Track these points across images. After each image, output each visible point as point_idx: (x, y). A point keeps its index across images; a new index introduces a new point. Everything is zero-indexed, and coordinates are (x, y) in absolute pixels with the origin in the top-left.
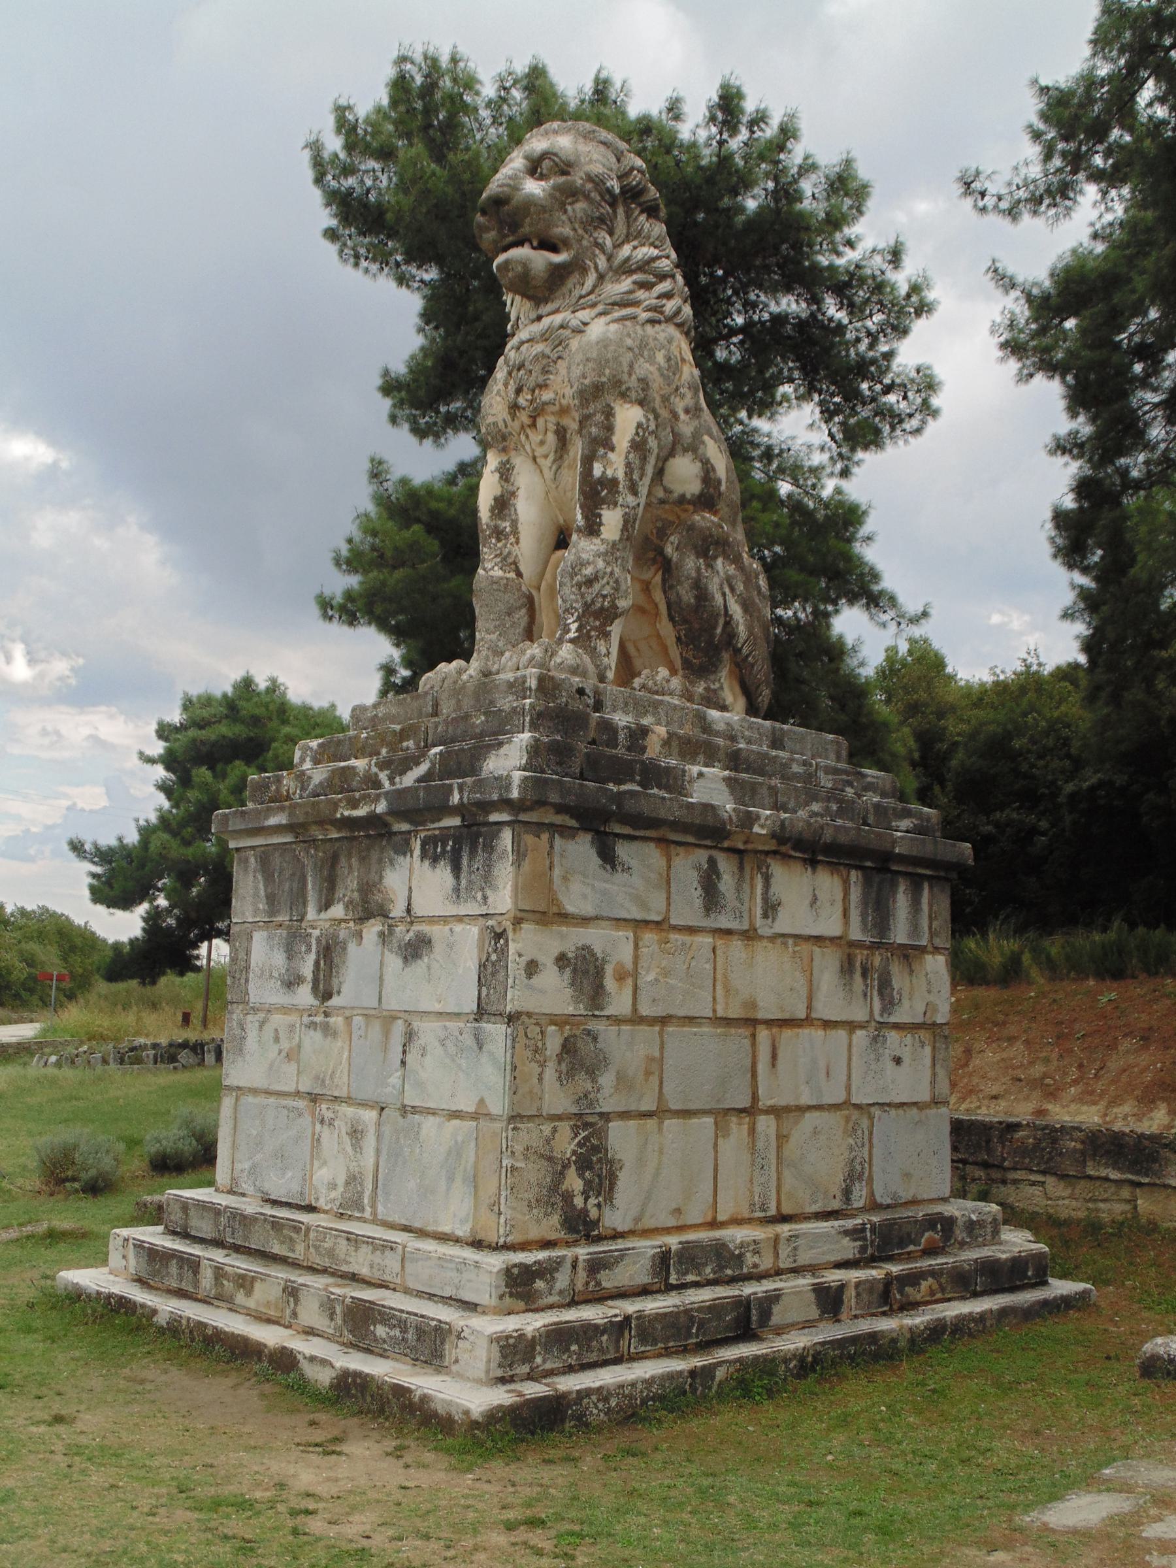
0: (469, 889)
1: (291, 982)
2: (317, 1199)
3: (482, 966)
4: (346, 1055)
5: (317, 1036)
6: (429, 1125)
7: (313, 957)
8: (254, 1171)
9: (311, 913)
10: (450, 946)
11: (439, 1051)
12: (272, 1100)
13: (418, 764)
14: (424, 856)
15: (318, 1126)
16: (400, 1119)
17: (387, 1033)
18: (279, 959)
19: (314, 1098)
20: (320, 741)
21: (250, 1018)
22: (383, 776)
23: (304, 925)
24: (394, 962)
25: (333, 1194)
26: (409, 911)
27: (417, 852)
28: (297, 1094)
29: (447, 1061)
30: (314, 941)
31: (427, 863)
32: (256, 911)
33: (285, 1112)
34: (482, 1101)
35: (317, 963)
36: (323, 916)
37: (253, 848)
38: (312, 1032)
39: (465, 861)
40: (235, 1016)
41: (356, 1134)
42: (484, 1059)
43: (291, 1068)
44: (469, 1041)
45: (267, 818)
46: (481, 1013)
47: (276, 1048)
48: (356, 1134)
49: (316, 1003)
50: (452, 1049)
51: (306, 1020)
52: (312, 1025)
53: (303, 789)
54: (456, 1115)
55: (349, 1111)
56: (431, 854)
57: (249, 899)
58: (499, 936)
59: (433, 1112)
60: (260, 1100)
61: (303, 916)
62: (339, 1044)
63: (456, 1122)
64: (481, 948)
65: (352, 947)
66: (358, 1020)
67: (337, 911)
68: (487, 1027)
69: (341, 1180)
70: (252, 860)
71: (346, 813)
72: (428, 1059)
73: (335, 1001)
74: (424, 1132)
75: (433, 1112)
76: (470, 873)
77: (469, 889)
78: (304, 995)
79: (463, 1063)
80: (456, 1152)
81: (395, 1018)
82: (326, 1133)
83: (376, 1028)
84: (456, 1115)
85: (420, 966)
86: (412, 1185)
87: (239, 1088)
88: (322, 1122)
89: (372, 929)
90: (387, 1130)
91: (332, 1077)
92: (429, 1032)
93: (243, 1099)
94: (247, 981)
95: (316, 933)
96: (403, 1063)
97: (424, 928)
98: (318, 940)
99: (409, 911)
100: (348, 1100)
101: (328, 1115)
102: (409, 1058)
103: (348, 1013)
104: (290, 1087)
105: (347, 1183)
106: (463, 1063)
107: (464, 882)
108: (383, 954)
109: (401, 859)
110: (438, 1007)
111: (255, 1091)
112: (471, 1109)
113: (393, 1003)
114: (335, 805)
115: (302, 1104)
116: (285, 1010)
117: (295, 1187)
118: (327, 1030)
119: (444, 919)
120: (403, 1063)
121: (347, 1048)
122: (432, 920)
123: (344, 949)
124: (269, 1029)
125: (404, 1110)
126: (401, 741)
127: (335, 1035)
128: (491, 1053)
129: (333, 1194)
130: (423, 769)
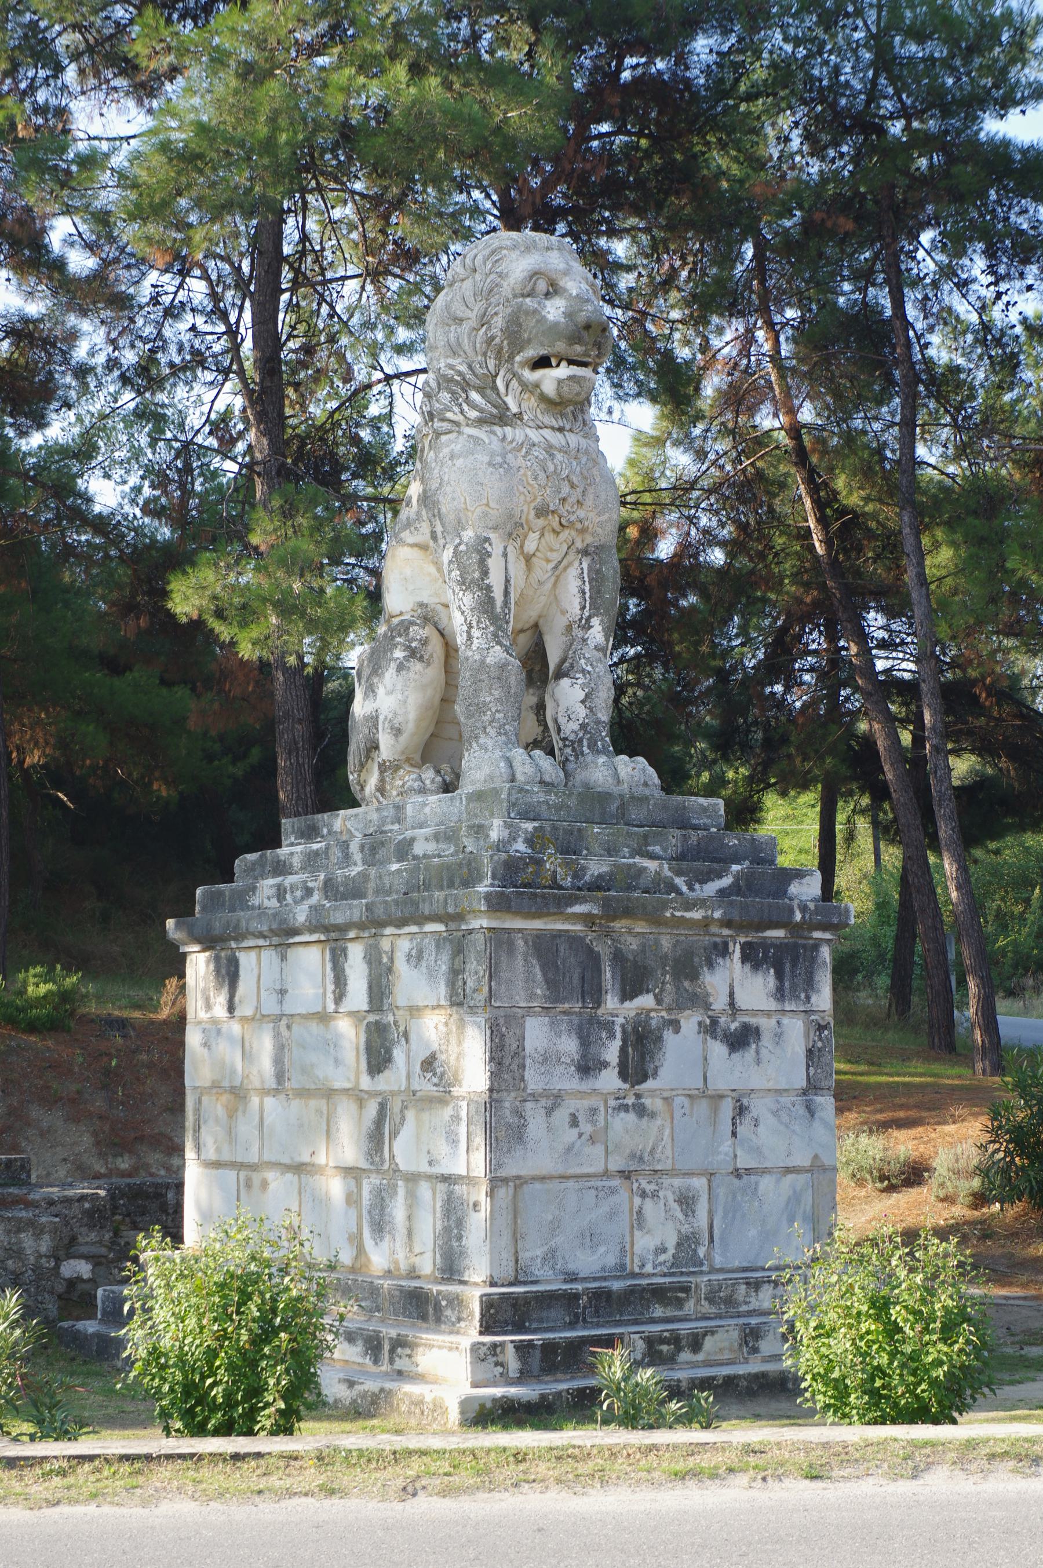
0: (794, 987)
1: (588, 1067)
2: (643, 1266)
3: (810, 1053)
4: (667, 1132)
5: (631, 1117)
6: (766, 1183)
7: (617, 1043)
8: (551, 1255)
9: (611, 1002)
10: (779, 1036)
11: (771, 1120)
12: (570, 1184)
13: (720, 877)
14: (745, 959)
15: (637, 1201)
16: (736, 1181)
17: (715, 1111)
18: (569, 1045)
19: (626, 1175)
20: (536, 824)
21: (529, 1105)
22: (680, 882)
23: (600, 1012)
24: (718, 1049)
25: (662, 1258)
26: (732, 1004)
27: (737, 954)
28: (606, 1174)
29: (782, 1128)
30: (618, 1030)
31: (748, 966)
32: (532, 996)
33: (593, 1192)
34: (816, 1157)
35: (623, 1050)
36: (627, 1004)
37: (520, 930)
38: (622, 1114)
39: (788, 968)
40: (507, 1104)
41: (686, 1202)
42: (816, 1124)
43: (598, 1150)
44: (802, 1111)
45: (571, 905)
46: (812, 1087)
47: (575, 1131)
48: (686, 1202)
49: (627, 1086)
50: (785, 1118)
51: (612, 1103)
52: (625, 1108)
53: (575, 876)
54: (789, 1170)
55: (677, 1182)
56: (752, 956)
57: (520, 984)
58: (821, 1028)
59: (765, 1171)
60: (555, 1185)
61: (598, 1003)
62: (659, 1122)
63: (790, 1177)
64: (807, 1035)
65: (668, 1035)
66: (679, 1101)
67: (646, 1001)
68: (819, 1099)
69: (671, 1243)
70: (521, 943)
71: (678, 914)
72: (761, 1129)
73: (650, 1084)
74: (762, 1187)
75: (765, 1171)
76: (793, 976)
77: (794, 987)
78: (609, 1080)
79: (797, 1128)
80: (795, 1198)
81: (722, 1097)
82: (649, 1205)
83: (703, 1107)
84: (789, 1170)
85: (750, 1052)
86: (753, 1233)
87: (519, 1177)
88: (643, 1194)
89: (690, 1021)
90: (721, 1192)
91: (652, 1152)
92: (759, 1107)
93: (526, 1189)
94: (523, 1066)
95: (620, 1020)
96: (734, 1134)
97: (753, 1021)
98: (623, 1026)
99: (732, 1004)
100: (673, 1173)
101: (650, 1188)
102: (740, 1129)
103: (666, 1094)
104: (598, 1167)
105: (679, 1245)
106: (797, 1128)
107: (787, 984)
108: (705, 1041)
109: (720, 960)
110: (771, 1085)
111: (543, 1179)
112: (807, 1163)
113: (720, 1083)
114: (664, 905)
115: (616, 1182)
116: (582, 1095)
117: (611, 1260)
118: (641, 1111)
119: (768, 1014)
120: (734, 1134)
121: (668, 1124)
122: (755, 1013)
123: (659, 1039)
124: (561, 1115)
125: (737, 1173)
126: (647, 845)
127: (653, 1115)
128: (821, 1119)
129: (662, 1258)
130: (726, 881)
